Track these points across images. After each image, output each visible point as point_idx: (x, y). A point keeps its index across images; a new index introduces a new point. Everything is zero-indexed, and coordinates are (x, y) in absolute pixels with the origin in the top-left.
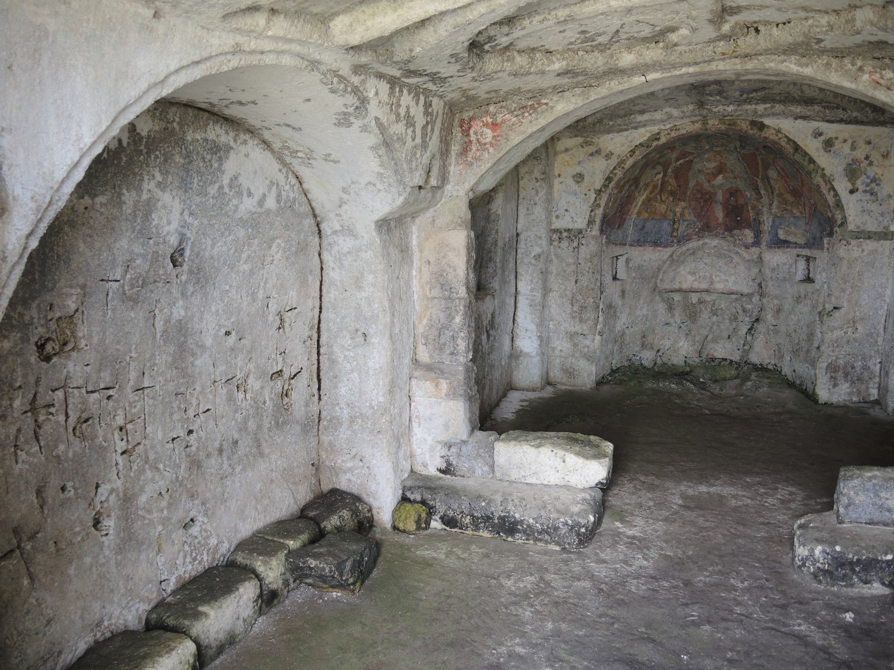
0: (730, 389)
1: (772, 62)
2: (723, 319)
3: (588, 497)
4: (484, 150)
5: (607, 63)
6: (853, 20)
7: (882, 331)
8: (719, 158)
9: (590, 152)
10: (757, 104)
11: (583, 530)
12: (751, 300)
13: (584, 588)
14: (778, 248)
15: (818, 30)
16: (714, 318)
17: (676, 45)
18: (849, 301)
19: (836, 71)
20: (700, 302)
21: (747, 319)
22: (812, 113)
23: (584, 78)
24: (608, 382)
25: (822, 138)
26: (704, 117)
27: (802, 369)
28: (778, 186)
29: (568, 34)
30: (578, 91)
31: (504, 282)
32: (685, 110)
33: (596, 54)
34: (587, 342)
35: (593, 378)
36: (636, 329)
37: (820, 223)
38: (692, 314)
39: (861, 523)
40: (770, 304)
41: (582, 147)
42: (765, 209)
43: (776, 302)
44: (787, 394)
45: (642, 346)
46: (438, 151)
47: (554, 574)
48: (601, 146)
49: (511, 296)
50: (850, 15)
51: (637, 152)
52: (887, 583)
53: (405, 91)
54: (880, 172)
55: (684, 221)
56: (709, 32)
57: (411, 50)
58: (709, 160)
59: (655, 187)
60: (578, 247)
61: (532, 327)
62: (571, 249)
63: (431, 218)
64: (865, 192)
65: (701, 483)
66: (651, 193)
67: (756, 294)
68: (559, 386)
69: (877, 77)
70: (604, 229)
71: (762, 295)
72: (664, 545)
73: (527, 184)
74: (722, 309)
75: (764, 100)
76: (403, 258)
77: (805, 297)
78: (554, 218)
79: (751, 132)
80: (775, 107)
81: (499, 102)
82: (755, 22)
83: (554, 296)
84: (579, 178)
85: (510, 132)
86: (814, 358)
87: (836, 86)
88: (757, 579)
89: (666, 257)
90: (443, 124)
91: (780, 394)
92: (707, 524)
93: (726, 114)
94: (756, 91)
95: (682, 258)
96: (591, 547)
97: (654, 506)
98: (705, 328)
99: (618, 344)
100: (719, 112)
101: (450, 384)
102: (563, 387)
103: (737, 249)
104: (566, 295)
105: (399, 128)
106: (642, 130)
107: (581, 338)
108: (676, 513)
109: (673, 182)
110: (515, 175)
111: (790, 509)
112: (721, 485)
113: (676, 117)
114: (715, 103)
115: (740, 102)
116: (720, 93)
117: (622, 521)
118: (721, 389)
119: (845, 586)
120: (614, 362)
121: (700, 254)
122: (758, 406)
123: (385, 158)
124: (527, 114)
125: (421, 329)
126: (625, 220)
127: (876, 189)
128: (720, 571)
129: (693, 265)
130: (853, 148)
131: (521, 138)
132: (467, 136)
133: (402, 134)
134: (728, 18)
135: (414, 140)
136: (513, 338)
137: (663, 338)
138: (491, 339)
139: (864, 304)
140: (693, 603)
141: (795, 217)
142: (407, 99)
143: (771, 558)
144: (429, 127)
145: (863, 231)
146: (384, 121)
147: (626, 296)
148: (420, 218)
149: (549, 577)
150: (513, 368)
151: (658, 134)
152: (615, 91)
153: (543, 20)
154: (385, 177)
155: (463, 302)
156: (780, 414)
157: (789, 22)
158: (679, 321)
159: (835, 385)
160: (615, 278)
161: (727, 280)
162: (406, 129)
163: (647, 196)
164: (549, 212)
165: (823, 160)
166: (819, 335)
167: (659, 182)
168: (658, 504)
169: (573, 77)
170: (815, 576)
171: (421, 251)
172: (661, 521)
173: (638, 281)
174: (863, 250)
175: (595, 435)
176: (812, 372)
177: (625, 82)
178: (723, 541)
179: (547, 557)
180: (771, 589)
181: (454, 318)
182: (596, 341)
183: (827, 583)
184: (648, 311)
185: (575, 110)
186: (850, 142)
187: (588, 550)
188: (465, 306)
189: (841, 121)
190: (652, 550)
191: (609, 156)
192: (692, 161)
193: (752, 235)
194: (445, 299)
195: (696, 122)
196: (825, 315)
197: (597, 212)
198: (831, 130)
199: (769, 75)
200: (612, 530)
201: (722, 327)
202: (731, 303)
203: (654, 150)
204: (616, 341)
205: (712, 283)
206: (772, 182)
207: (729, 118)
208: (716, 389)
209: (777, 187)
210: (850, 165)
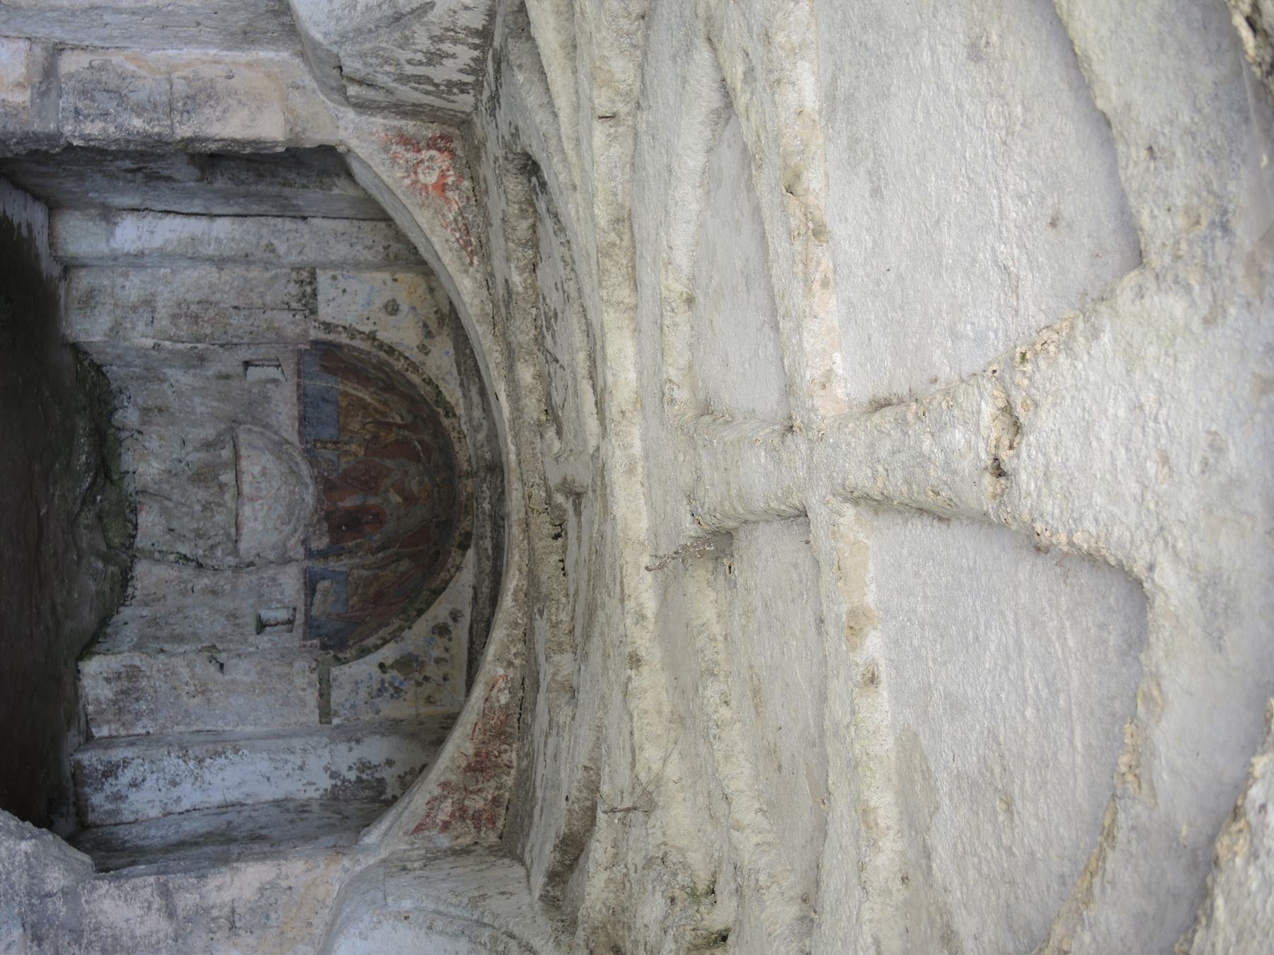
1: (520, 557)
2: (199, 520)
4: (407, 171)
5: (521, 347)
6: (562, 651)
7: (195, 728)
9: (429, 323)
10: (492, 538)
12: (228, 554)
14: (305, 583)
15: (553, 610)
16: (198, 508)
17: (542, 436)
19: (508, 635)
20: (222, 487)
21: (201, 552)
22: (481, 606)
23: (504, 316)
24: (78, 361)
25: (450, 622)
26: (476, 473)
27: (130, 634)
29: (554, 292)
30: (489, 308)
31: (227, 197)
33: (533, 332)
34: (141, 327)
35: (83, 338)
36: (171, 399)
38: (203, 476)
40: (223, 581)
41: (436, 312)
42: (357, 560)
43: (228, 587)
44: (88, 618)
45: (144, 409)
46: (398, 100)
48: (438, 338)
49: (206, 207)
50: (568, 647)
51: (429, 388)
53: (476, 53)
54: (409, 696)
55: (338, 456)
56: (554, 480)
57: (520, 66)
58: (421, 483)
59: (383, 414)
60: (289, 309)
61: (157, 242)
62: (286, 299)
63: (301, 84)
64: (383, 681)
66: (376, 410)
67: (238, 560)
68: (63, 285)
69: (501, 684)
70: (320, 346)
71: (236, 569)
73: (371, 233)
74: (213, 516)
76: (233, 34)
77: (237, 625)
78: (332, 273)
79: (457, 534)
80: (488, 560)
81: (475, 196)
82: (566, 534)
83: (212, 274)
84: (392, 308)
85: (432, 211)
86: (147, 647)
89: (284, 434)
90: (439, 109)
91: (88, 609)
95: (284, 457)
98: (182, 496)
100: (482, 492)
101: (24, 108)
102: (62, 292)
103: (301, 529)
104: (214, 293)
105: (422, 41)
106: (459, 393)
107: (147, 316)
109: (392, 437)
110: (377, 214)
113: (475, 438)
114: (493, 486)
118: (86, 527)
120: (114, 368)
121: (292, 480)
122: (63, 581)
123: (377, 14)
124: (458, 235)
125: (117, 59)
126: (336, 375)
127: (387, 695)
129: (275, 472)
130: (438, 661)
131: (425, 226)
132: (428, 145)
133: (413, 43)
134: (571, 500)
135: (409, 62)
136: (138, 210)
137: (161, 438)
138: (129, 176)
139: (231, 700)
141: (347, 600)
142: (465, 55)
144: (431, 88)
145: (330, 686)
146: (430, 16)
147: (222, 382)
148: (302, 66)
150: (87, 212)
151: (455, 415)
152: (488, 358)
153: (564, 261)
154: (350, 11)
155: (167, 131)
157: (564, 575)
158: (190, 458)
159: (108, 680)
160: (247, 364)
161: (256, 520)
162: (421, 51)
163: (370, 404)
164: (341, 265)
165: (422, 626)
167: (390, 420)
169: (504, 301)
171: (249, 65)
174: (304, 690)
176: (125, 647)
177: (499, 372)
181: (139, 116)
182: (143, 340)
184: (201, 413)
185: (464, 304)
186: (446, 655)
188: (159, 134)
191: (424, 349)
192: (419, 461)
193: (322, 547)
194: (170, 103)
195: (470, 464)
196: (209, 654)
197: (344, 335)
201: (186, 519)
202: (224, 528)
203: (432, 410)
204: (148, 370)
205: (252, 500)
206: (393, 566)
207: (475, 505)
210: (417, 659)
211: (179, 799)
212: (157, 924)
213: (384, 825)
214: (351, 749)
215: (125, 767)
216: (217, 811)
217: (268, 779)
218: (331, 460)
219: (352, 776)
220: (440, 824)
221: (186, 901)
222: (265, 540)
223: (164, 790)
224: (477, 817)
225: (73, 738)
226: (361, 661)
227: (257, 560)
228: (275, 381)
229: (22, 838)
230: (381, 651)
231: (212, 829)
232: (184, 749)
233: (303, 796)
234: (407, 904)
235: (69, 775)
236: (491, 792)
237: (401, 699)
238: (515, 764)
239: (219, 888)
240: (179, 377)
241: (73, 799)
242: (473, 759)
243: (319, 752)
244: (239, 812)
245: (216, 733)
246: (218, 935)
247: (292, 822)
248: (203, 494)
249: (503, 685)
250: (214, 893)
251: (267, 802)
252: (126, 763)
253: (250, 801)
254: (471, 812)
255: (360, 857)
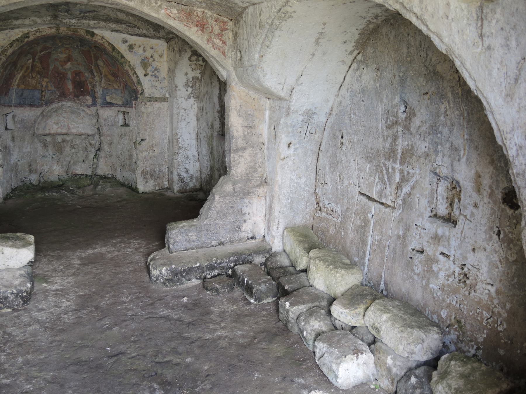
0: (88, 191)
3: (23, 272)
7: (167, 150)
8: (67, 52)
10: (89, 20)
11: (25, 294)
13: (35, 329)
14: (107, 107)
16: (73, 150)
18: (149, 136)
19: (147, 6)
20: (63, 141)
21: (93, 149)
22: (121, 29)
24: (11, 197)
25: (127, 44)
26: (57, 25)
27: (128, 175)
28: (104, 70)
32: (45, 20)
36: (25, 161)
37: (129, 93)
38: (59, 149)
39: (181, 251)
40: (106, 140)
42: (97, 84)
43: (109, 138)
44: (121, 190)
45: (30, 172)
47: (12, 327)
51: (15, 45)
52: (199, 278)
54: (158, 64)
55: (48, 90)
58: (61, 53)
59: (28, 68)
64: (152, 75)
65: (88, 249)
66: (25, 72)
67: (96, 135)
71: (100, 135)
72: (77, 289)
74: (77, 145)
75: (94, 18)
79: (87, 37)
80: (100, 23)
86: (134, 168)
87: (147, 15)
88: (134, 294)
89: (39, 114)
91: (117, 190)
92: (99, 271)
93: (71, 25)
94: (89, 12)
95: (49, 114)
96: (32, 303)
97: (64, 268)
98: (69, 157)
99: (14, 172)
100: (67, 23)
103: (83, 108)
106: (16, 31)
108: (78, 269)
109: (39, 65)
111: (140, 252)
112: (100, 247)
113: (39, 24)
114: (64, 17)
115: (80, 18)
116: (67, 11)
117: (47, 282)
118: (83, 193)
119: (179, 285)
120: (13, 184)
121: (60, 111)
126: (9, 89)
128: (113, 295)
129: (56, 118)
130: (144, 51)
137: (43, 165)
139: (156, 137)
140: (104, 318)
141: (115, 89)
143: (138, 281)
145: (153, 97)
147: (16, 140)
149: (9, 330)
151: (28, 33)
156: (120, 202)
158: (51, 154)
159: (147, 182)
160: (6, 129)
161: (78, 127)
165: (128, 56)
166: (135, 155)
167: (31, 65)
168: (66, 266)
170: (164, 283)
172: (71, 276)
173: (22, 130)
174: (154, 108)
175: (20, 232)
176: (134, 176)
178: (110, 279)
179: (4, 318)
180: (143, 297)
183: (171, 286)
184: (31, 149)
186: (142, 47)
187: (30, 306)
189: (137, 35)
190: (71, 295)
192: (50, 53)
193: (91, 99)
195: (53, 28)
196: (137, 144)
198: (132, 39)
199: (108, 3)
200: (42, 290)
201: (79, 155)
202: (82, 140)
204: (12, 170)
205: (69, 129)
206: (100, 68)
207: (73, 27)
208: (80, 192)
209: (103, 71)
210: (143, 60)
211: (194, 156)
212: (247, 154)
213: (220, 69)
214: (180, 90)
215: (180, 175)
216: (199, 142)
217: (188, 123)
218: (50, 94)
219: (190, 90)
220: (223, 45)
221: (240, 143)
222: (87, 123)
223: (190, 161)
224: (222, 29)
225: (169, 194)
226: (143, 84)
227: (97, 127)
228: (14, 117)
229: (214, 199)
230: (139, 75)
231: (206, 143)
232: (175, 154)
233: (196, 108)
234: (257, 56)
235: (182, 194)
236: (213, 22)
237: (160, 68)
238: (203, 10)
239: (237, 131)
240: (15, 158)
241: (191, 193)
242: (199, 28)
243: (180, 102)
244: (200, 134)
245: (169, 143)
246: (254, 132)
247: (206, 113)
248: (67, 149)
249: (169, 11)
250: (239, 133)
251: (197, 124)
252: (179, 175)
253: (196, 130)
254: (220, 32)
255: (232, 78)
